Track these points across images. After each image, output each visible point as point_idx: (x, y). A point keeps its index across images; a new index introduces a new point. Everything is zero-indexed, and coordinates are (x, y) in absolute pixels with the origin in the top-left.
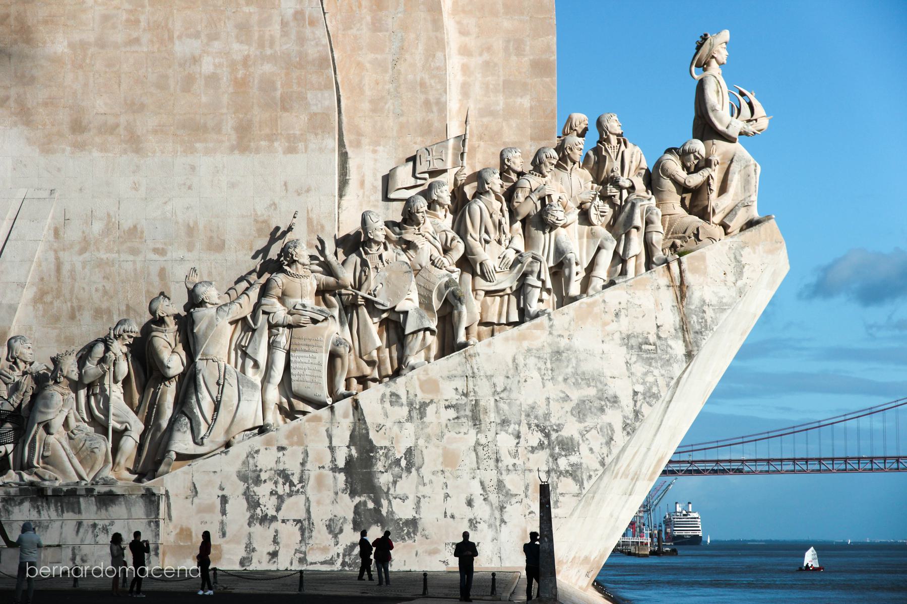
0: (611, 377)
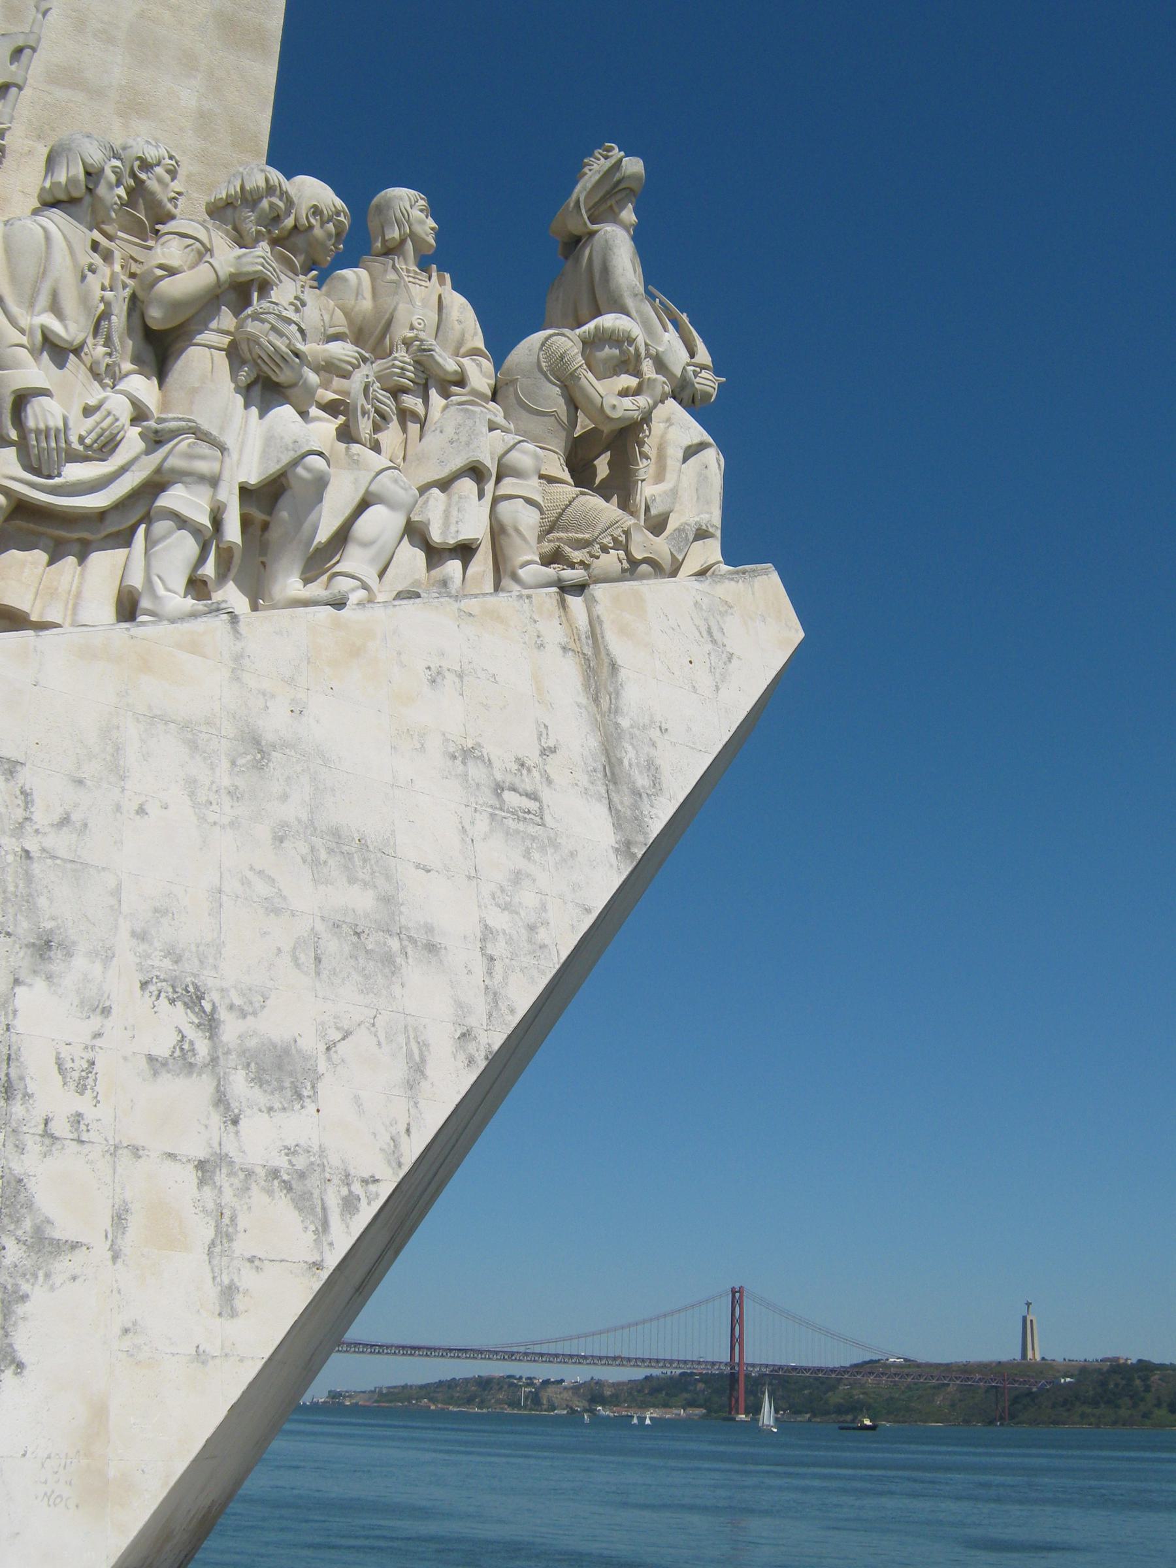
0: (418, 866)
